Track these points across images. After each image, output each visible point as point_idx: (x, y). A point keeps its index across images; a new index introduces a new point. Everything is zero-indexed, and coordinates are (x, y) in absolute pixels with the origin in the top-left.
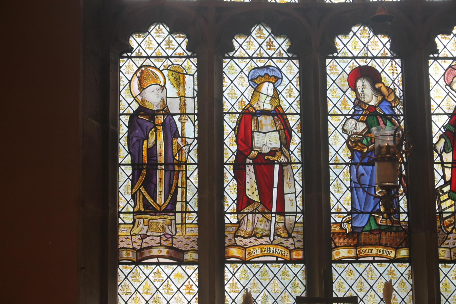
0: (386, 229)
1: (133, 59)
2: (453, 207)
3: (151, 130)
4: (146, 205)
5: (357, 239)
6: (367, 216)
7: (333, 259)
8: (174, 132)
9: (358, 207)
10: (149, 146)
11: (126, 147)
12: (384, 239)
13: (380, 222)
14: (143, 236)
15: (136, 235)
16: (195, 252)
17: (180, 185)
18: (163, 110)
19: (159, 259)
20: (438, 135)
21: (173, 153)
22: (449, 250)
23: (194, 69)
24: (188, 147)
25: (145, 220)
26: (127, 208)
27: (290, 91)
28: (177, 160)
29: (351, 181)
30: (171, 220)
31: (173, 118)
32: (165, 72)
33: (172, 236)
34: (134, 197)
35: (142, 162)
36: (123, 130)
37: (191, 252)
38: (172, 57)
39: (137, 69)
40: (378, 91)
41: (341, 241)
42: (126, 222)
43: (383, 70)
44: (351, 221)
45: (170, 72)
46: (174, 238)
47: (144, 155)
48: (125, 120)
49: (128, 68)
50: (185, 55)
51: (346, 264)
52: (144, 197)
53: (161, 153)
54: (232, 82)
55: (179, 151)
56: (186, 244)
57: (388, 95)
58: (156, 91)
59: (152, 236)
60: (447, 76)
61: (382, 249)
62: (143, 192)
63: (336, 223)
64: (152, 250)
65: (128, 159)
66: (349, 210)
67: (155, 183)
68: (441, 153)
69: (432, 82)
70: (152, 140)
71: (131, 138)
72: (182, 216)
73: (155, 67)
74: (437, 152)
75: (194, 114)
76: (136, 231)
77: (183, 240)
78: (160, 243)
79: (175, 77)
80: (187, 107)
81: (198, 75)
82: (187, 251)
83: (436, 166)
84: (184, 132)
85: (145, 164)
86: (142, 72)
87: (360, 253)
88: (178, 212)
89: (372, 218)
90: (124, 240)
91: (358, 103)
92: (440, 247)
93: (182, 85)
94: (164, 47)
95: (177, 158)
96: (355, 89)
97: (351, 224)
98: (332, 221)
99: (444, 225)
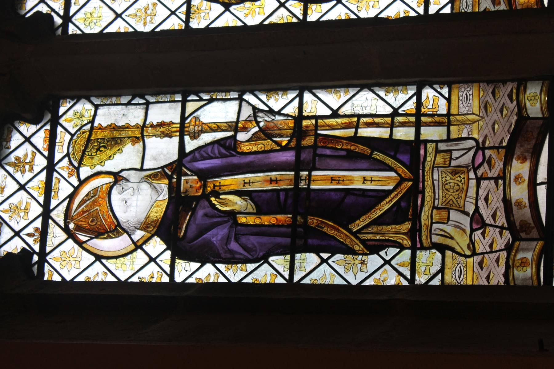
1: (48, 249)
3: (213, 206)
4: (394, 216)
8: (223, 151)
10: (251, 211)
11: (250, 267)
14: (477, 223)
15: (472, 244)
16: (522, 88)
17: (350, 132)
18: (170, 178)
19: (539, 181)
21: (272, 151)
23: (84, 108)
24: (260, 114)
25: (436, 218)
26: (402, 265)
28: (289, 141)
30: (437, 151)
31: (191, 152)
32: (85, 172)
33: (480, 147)
34: (374, 248)
35: (288, 226)
36: (208, 273)
37: (522, 98)
38: (50, 158)
39: (70, 241)
42: (437, 267)
45: (86, 161)
46: (484, 142)
47: (273, 221)
48: (185, 271)
49: (69, 263)
50: (48, 127)
52: (378, 222)
53: (271, 181)
54: (118, 16)
55: (269, 136)
56: (501, 111)
58: (125, 195)
59: (477, 200)
62: (362, 224)
64: (513, 201)
65: (280, 262)
67: (343, 194)
70: (237, 203)
71: (229, 256)
72: (428, 125)
73: (71, 197)
75: (184, 103)
76: (461, 242)
77: (489, 120)
78: (496, 179)
79: (98, 150)
80: (167, 120)
81: (97, 96)
82: (521, 108)
84: (223, 126)
85: (294, 219)
86: (79, 228)
88: (418, 133)
90: (484, 274)
93: (116, 134)
94: (28, 175)
95: (284, 141)
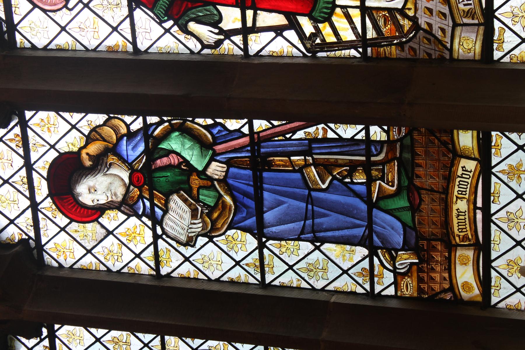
0: (408, 178)
2: (350, 11)
5: (434, 243)
6: (379, 216)
7: (480, 299)
9: (359, 232)
12: (431, 180)
13: (393, 186)
20: (182, 37)
22: (458, 29)
27: (116, 343)
29: (299, 239)
40: (99, 164)
41: (437, 276)
43: (53, 147)
44: (392, 253)
51: (493, 274)
57: (104, 140)
60: (46, 4)
61: (457, 189)
63: (396, 283)
66: (366, 252)
68: (221, 31)
69: (63, 40)
74: (219, 43)
83: (253, 49)
87: (465, 238)
89: (382, 204)
91: (127, 206)
92: (451, 50)
96: (99, 211)
97: (397, 251)
98: (391, 291)
99: (396, 38)
